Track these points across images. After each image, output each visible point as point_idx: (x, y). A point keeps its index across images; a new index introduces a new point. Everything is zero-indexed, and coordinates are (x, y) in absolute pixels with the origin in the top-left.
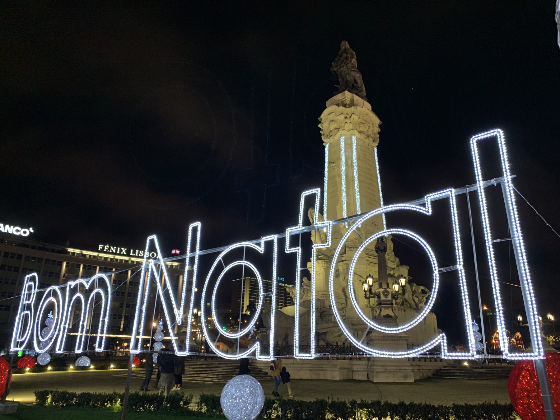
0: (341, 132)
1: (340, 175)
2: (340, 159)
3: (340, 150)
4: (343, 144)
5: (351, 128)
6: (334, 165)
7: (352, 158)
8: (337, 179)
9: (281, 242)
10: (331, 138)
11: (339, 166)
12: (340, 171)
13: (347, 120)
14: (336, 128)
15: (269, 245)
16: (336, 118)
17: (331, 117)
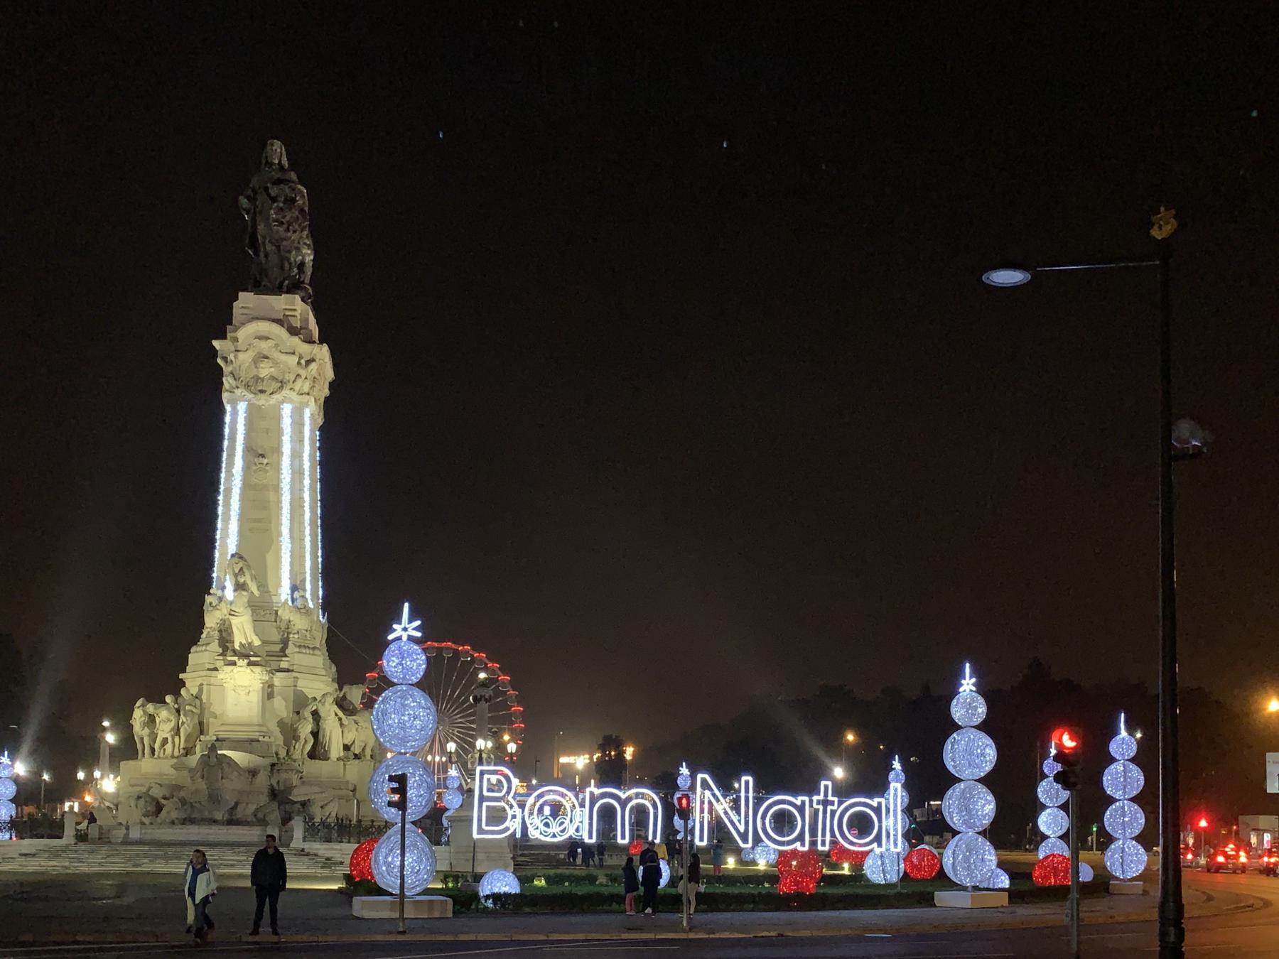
0: (286, 392)
1: (277, 489)
2: (278, 451)
3: (280, 432)
4: (286, 423)
5: (306, 389)
6: (265, 461)
7: (301, 457)
8: (272, 496)
9: (811, 801)
10: (261, 396)
11: (278, 470)
12: (279, 480)
13: (303, 373)
14: (273, 378)
15: (803, 802)
16: (276, 355)
17: (264, 346)
